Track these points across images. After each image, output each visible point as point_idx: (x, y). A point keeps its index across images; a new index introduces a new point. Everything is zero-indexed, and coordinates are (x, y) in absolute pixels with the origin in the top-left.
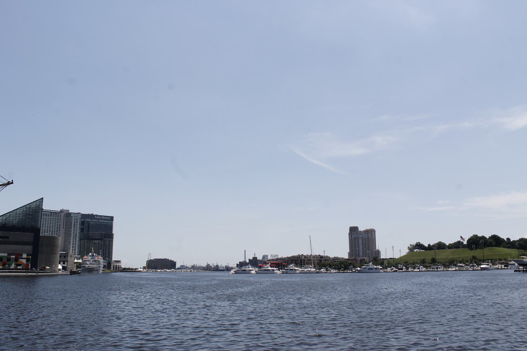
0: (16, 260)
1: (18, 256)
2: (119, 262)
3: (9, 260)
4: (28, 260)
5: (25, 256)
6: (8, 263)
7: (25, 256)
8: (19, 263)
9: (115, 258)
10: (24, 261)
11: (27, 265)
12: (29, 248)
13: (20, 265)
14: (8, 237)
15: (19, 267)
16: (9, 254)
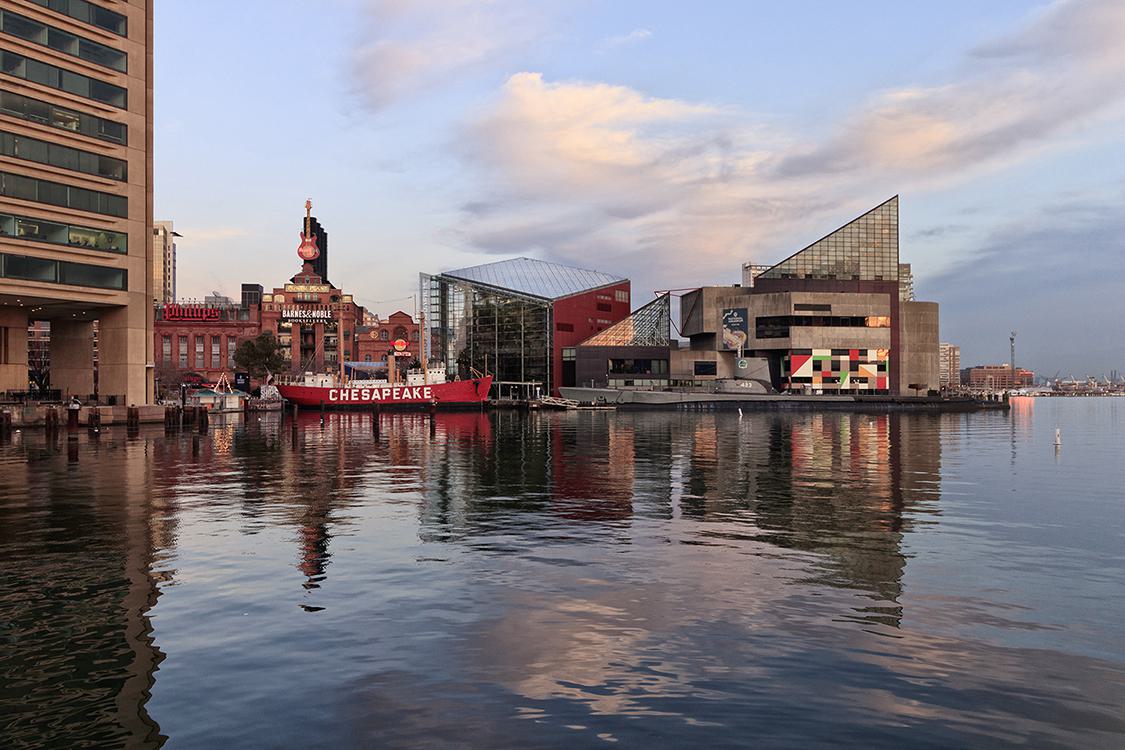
0: (854, 366)
1: (858, 358)
3: (836, 366)
4: (881, 368)
7: (872, 355)
8: (860, 374)
10: (872, 370)
11: (881, 380)
13: (864, 380)
14: (828, 308)
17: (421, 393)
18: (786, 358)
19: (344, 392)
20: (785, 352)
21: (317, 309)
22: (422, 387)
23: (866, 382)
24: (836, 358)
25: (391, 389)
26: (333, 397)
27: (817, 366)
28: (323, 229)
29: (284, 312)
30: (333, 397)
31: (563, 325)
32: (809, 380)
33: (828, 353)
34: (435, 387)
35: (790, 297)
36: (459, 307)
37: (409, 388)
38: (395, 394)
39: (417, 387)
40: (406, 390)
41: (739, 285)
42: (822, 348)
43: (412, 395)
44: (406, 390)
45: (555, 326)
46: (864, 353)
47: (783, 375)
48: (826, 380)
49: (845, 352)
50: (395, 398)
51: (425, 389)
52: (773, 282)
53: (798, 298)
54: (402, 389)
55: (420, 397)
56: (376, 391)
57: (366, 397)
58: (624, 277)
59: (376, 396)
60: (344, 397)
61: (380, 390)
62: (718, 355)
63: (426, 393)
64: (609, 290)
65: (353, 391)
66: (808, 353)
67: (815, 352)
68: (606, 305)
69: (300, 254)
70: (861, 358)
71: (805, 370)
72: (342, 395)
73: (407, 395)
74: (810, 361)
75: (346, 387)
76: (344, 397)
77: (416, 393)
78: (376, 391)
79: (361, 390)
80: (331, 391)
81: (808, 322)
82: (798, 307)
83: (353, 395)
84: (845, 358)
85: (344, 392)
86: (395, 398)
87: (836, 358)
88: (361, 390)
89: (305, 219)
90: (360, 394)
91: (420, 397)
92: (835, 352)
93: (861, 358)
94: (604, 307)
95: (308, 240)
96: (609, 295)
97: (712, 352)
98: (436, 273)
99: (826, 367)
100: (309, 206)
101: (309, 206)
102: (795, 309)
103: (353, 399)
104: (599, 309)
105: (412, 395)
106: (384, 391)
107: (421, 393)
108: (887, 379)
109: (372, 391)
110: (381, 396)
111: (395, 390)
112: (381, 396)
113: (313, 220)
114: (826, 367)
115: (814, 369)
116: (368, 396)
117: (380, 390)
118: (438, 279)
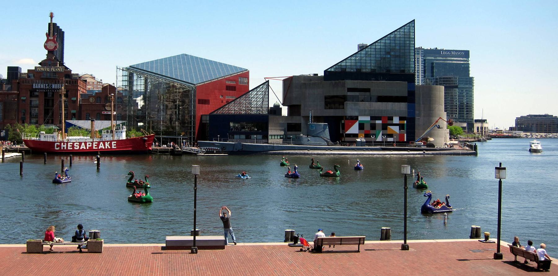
0: (384, 127)
1: (387, 122)
2: (483, 121)
3: (373, 127)
4: (401, 127)
5: (396, 120)
6: (372, 132)
7: (396, 120)
8: (389, 132)
9: (477, 115)
10: (396, 129)
11: (401, 136)
12: (402, 107)
13: (391, 136)
14: (368, 90)
15: (390, 139)
16: (373, 118)
17: (110, 145)
18: (343, 122)
20: (341, 118)
21: (56, 83)
22: (111, 141)
23: (392, 137)
24: (373, 122)
25: (92, 142)
27: (361, 126)
28: (61, 30)
29: (34, 85)
31: (203, 100)
32: (356, 136)
33: (368, 118)
34: (119, 142)
35: (344, 84)
36: (139, 85)
37: (103, 142)
38: (94, 145)
39: (108, 142)
40: (101, 143)
41: (317, 75)
42: (365, 115)
43: (105, 146)
44: (101, 143)
45: (197, 101)
46: (391, 119)
47: (341, 132)
48: (367, 136)
49: (379, 118)
50: (94, 148)
51: (113, 143)
52: (335, 75)
53: (350, 83)
54: (99, 143)
56: (83, 144)
57: (77, 148)
58: (53, 185)
59: (83, 146)
60: (64, 147)
61: (86, 143)
62: (302, 119)
64: (235, 78)
65: (69, 144)
66: (356, 118)
67: (361, 118)
68: (232, 87)
69: (46, 47)
70: (389, 122)
71: (354, 129)
73: (101, 146)
74: (356, 125)
75: (65, 141)
77: (107, 145)
78: (83, 144)
79: (74, 143)
81: (356, 99)
82: (350, 90)
83: (69, 146)
84: (379, 122)
85: (64, 144)
86: (94, 148)
87: (373, 122)
88: (74, 143)
89: (49, 24)
90: (73, 146)
92: (373, 118)
93: (389, 122)
94: (230, 88)
95: (51, 38)
96: (234, 80)
97: (298, 117)
98: (128, 66)
99: (367, 127)
100: (52, 16)
101: (52, 16)
102: (348, 91)
103: (69, 148)
104: (227, 89)
105: (105, 146)
106: (88, 143)
107: (110, 145)
108: (405, 135)
109: (80, 144)
110: (86, 147)
111: (94, 143)
112: (86, 147)
113: (55, 25)
114: (367, 127)
115: (359, 129)
117: (86, 143)
118: (128, 69)
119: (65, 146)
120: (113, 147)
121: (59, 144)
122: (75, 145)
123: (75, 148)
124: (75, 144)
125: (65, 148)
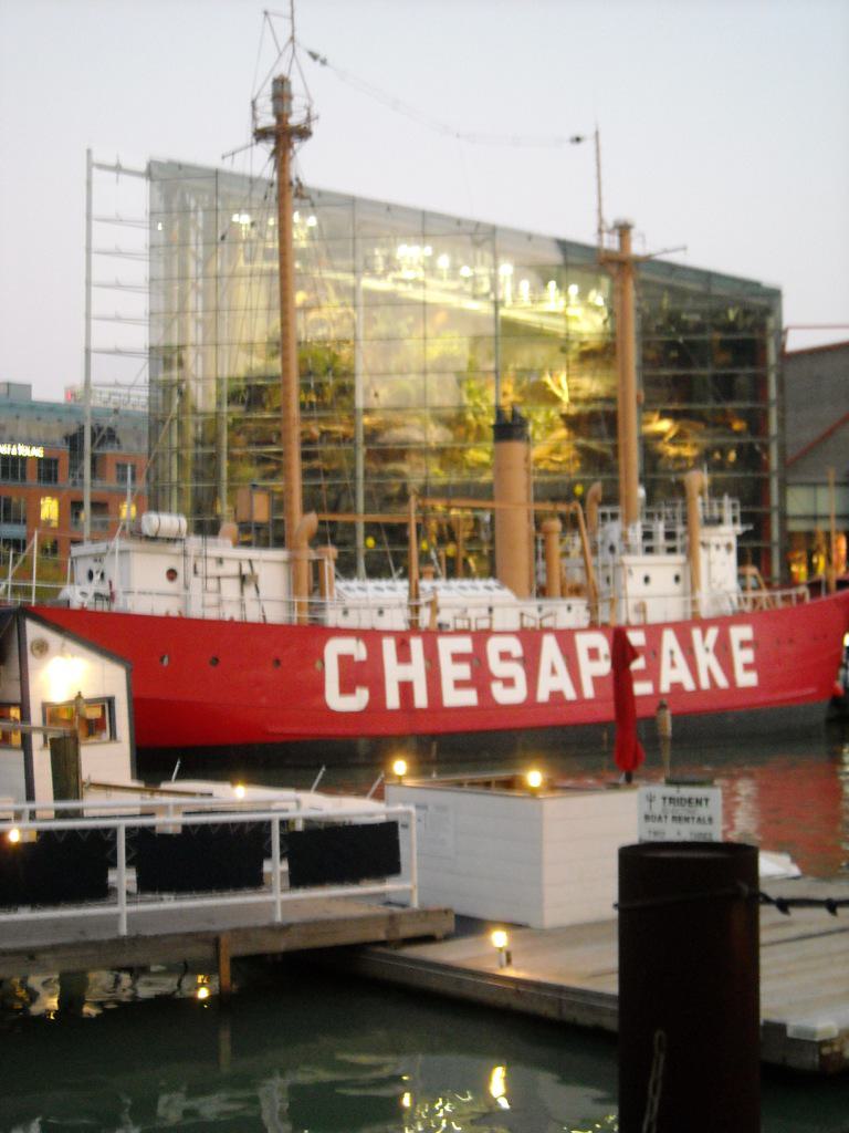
17: (723, 651)
19: (404, 655)
26: (347, 688)
30: (347, 688)
40: (669, 640)
55: (722, 682)
56: (550, 646)
59: (553, 681)
60: (406, 689)
63: (742, 656)
72: (394, 673)
76: (406, 689)
77: (707, 660)
78: (550, 646)
79: (481, 637)
80: (334, 649)
83: (451, 672)
85: (404, 655)
88: (481, 637)
91: (722, 682)
103: (454, 698)
106: (584, 642)
116: (517, 671)
119: (416, 672)
120: (747, 679)
121: (358, 650)
122: (497, 667)
123: (502, 695)
124: (494, 646)
125: (421, 699)
